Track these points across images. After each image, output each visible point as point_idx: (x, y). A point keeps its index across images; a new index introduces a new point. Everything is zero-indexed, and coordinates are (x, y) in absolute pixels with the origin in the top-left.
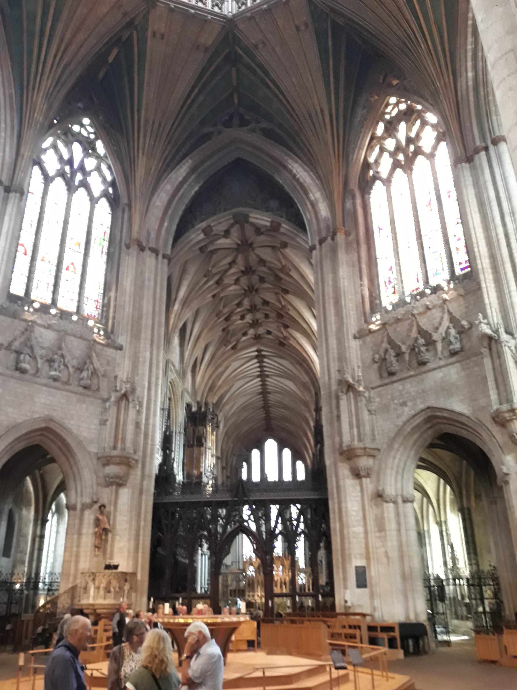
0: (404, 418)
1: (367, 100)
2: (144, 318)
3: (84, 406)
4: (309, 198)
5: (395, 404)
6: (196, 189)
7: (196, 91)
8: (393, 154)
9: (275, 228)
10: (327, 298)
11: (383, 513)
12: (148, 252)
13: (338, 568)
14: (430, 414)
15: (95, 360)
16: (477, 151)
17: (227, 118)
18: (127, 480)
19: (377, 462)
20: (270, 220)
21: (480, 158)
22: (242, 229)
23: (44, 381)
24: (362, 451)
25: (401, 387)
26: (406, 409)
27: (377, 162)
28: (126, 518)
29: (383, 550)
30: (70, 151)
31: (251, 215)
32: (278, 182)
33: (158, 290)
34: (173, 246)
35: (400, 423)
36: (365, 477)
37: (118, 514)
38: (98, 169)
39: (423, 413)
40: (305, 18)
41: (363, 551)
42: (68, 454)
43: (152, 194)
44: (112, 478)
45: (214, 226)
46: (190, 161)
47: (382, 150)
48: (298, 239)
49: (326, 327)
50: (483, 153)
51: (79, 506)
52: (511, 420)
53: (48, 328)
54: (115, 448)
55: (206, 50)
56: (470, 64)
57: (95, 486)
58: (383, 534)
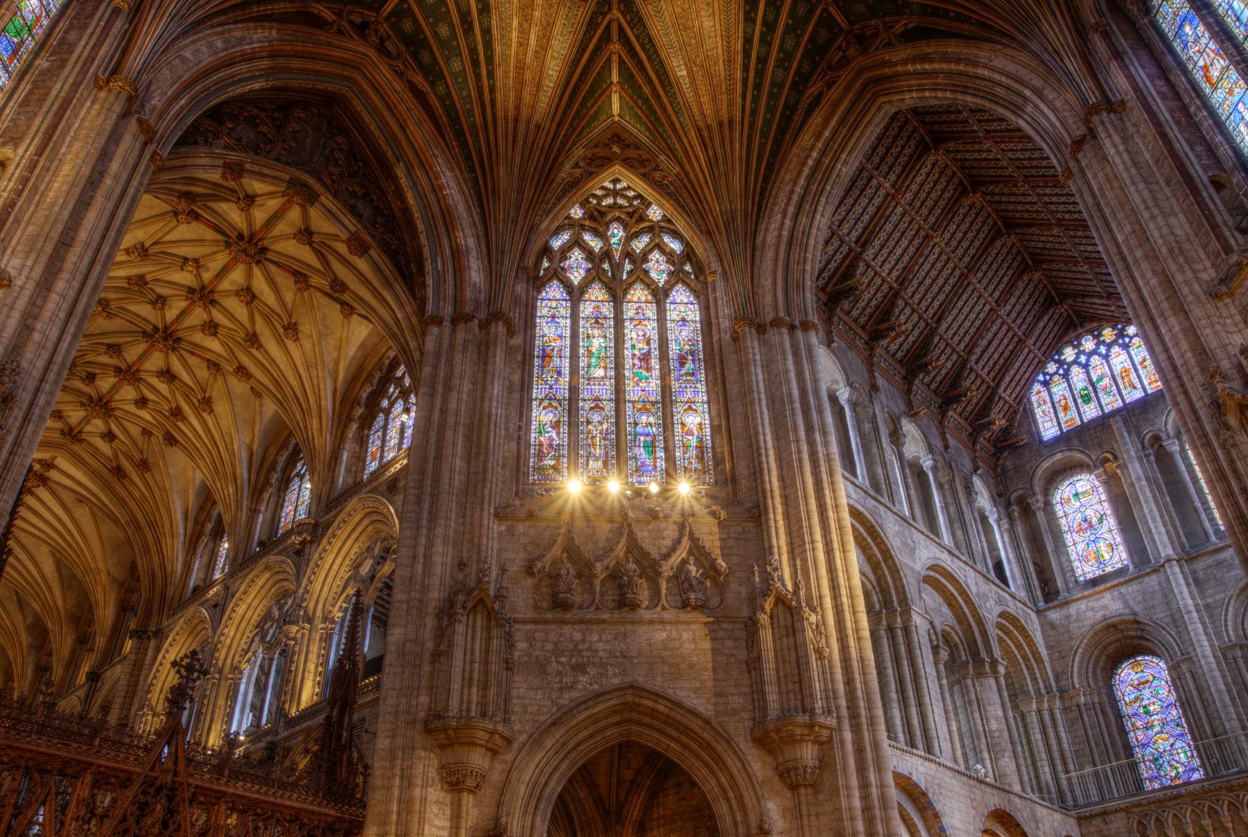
5: (558, 662)
6: (257, 86)
10: (451, 420)
14: (629, 698)
16: (777, 323)
17: (358, 20)
19: (498, 767)
21: (781, 334)
24: (486, 736)
26: (584, 679)
35: (565, 699)
36: (471, 791)
39: (617, 694)
46: (274, 32)
50: (785, 330)
52: (801, 741)
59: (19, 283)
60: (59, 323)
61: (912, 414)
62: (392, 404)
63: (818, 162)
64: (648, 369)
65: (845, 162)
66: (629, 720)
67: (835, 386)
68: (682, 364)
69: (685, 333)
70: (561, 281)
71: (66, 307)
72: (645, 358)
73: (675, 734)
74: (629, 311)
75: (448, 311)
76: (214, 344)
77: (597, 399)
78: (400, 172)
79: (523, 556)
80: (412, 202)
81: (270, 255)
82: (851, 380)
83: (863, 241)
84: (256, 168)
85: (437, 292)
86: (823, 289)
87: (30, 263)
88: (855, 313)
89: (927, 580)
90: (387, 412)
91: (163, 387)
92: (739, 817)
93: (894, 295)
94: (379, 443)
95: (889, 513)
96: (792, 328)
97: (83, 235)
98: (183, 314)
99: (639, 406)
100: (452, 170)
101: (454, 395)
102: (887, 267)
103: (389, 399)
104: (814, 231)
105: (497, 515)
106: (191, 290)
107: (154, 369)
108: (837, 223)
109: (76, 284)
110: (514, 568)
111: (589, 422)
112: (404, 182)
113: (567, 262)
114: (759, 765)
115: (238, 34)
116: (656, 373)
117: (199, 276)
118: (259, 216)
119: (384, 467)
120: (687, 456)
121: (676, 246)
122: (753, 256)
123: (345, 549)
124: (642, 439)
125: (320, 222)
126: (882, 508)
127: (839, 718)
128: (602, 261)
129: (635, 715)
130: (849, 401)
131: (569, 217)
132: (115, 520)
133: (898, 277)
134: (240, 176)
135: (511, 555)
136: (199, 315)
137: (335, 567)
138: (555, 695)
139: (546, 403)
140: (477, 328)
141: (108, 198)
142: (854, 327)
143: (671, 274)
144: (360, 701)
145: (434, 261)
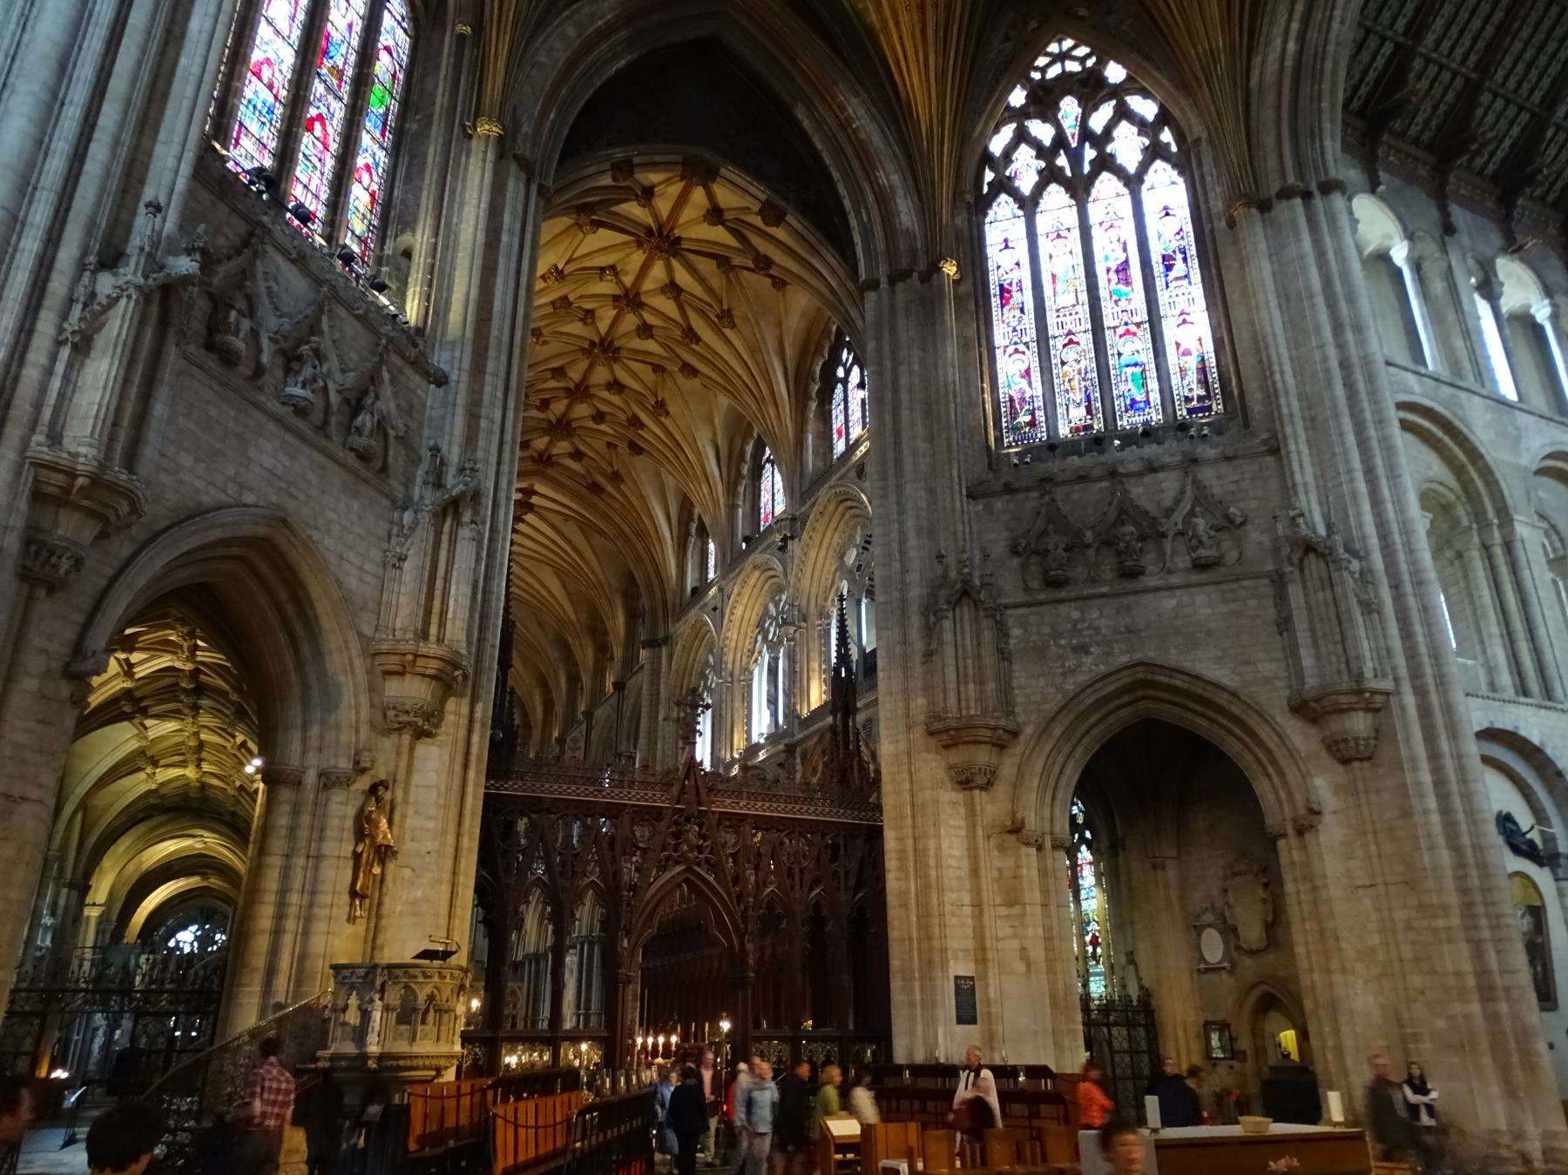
0: (1082, 678)
3: (356, 506)
5: (1058, 646)
6: (622, 63)
10: (905, 397)
11: (1018, 867)
13: (908, 979)
14: (1141, 676)
15: (387, 390)
16: (1286, 194)
18: (437, 726)
20: (763, 197)
21: (1292, 209)
23: (275, 406)
25: (1076, 615)
26: (1087, 661)
28: (431, 825)
29: (1015, 944)
31: (723, 171)
35: (1070, 686)
36: (983, 788)
37: (410, 811)
39: (1128, 672)
41: (970, 944)
42: (299, 629)
44: (407, 712)
50: (1298, 202)
51: (311, 778)
53: (293, 262)
54: (424, 634)
57: (364, 729)
58: (1016, 910)
59: (453, 377)
60: (499, 403)
61: (1512, 247)
62: (848, 372)
66: (1143, 698)
67: (1387, 243)
68: (1169, 268)
69: (1171, 225)
70: (1010, 194)
71: (501, 385)
72: (1123, 269)
73: (1199, 708)
74: (1095, 212)
75: (882, 271)
76: (651, 346)
77: (1070, 333)
78: (800, 113)
79: (1005, 534)
80: (819, 146)
81: (685, 245)
82: (1411, 228)
83: (1416, 29)
84: (645, 159)
85: (867, 252)
86: (1360, 114)
87: (457, 354)
88: (1413, 130)
89: (1541, 472)
90: (845, 382)
91: (615, 399)
92: (1283, 795)
93: (1473, 90)
94: (841, 417)
95: (1476, 399)
96: (1307, 196)
97: (497, 305)
98: (615, 321)
99: (1121, 330)
100: (857, 95)
101: (904, 368)
102: (1459, 51)
103: (844, 366)
104: (1331, 48)
105: (968, 496)
106: (616, 298)
107: (602, 382)
108: (1372, 15)
109: (504, 358)
110: (999, 549)
111: (1063, 363)
112: (807, 124)
113: (1013, 167)
114: (1300, 736)
115: (587, 10)
117: (620, 282)
118: (664, 206)
119: (851, 448)
121: (1146, 108)
122: (1247, 105)
123: (826, 541)
124: (1130, 370)
125: (726, 197)
126: (1463, 395)
127: (1396, 680)
128: (1056, 154)
129: (1151, 692)
130: (1409, 259)
131: (1008, 108)
132: (601, 532)
133: (1478, 63)
134: (631, 173)
135: (993, 536)
136: (630, 321)
137: (820, 560)
138: (1058, 680)
139: (1011, 349)
140: (918, 283)
141: (509, 257)
142: (1413, 150)
143: (1145, 150)
144: (859, 705)
145: (858, 215)
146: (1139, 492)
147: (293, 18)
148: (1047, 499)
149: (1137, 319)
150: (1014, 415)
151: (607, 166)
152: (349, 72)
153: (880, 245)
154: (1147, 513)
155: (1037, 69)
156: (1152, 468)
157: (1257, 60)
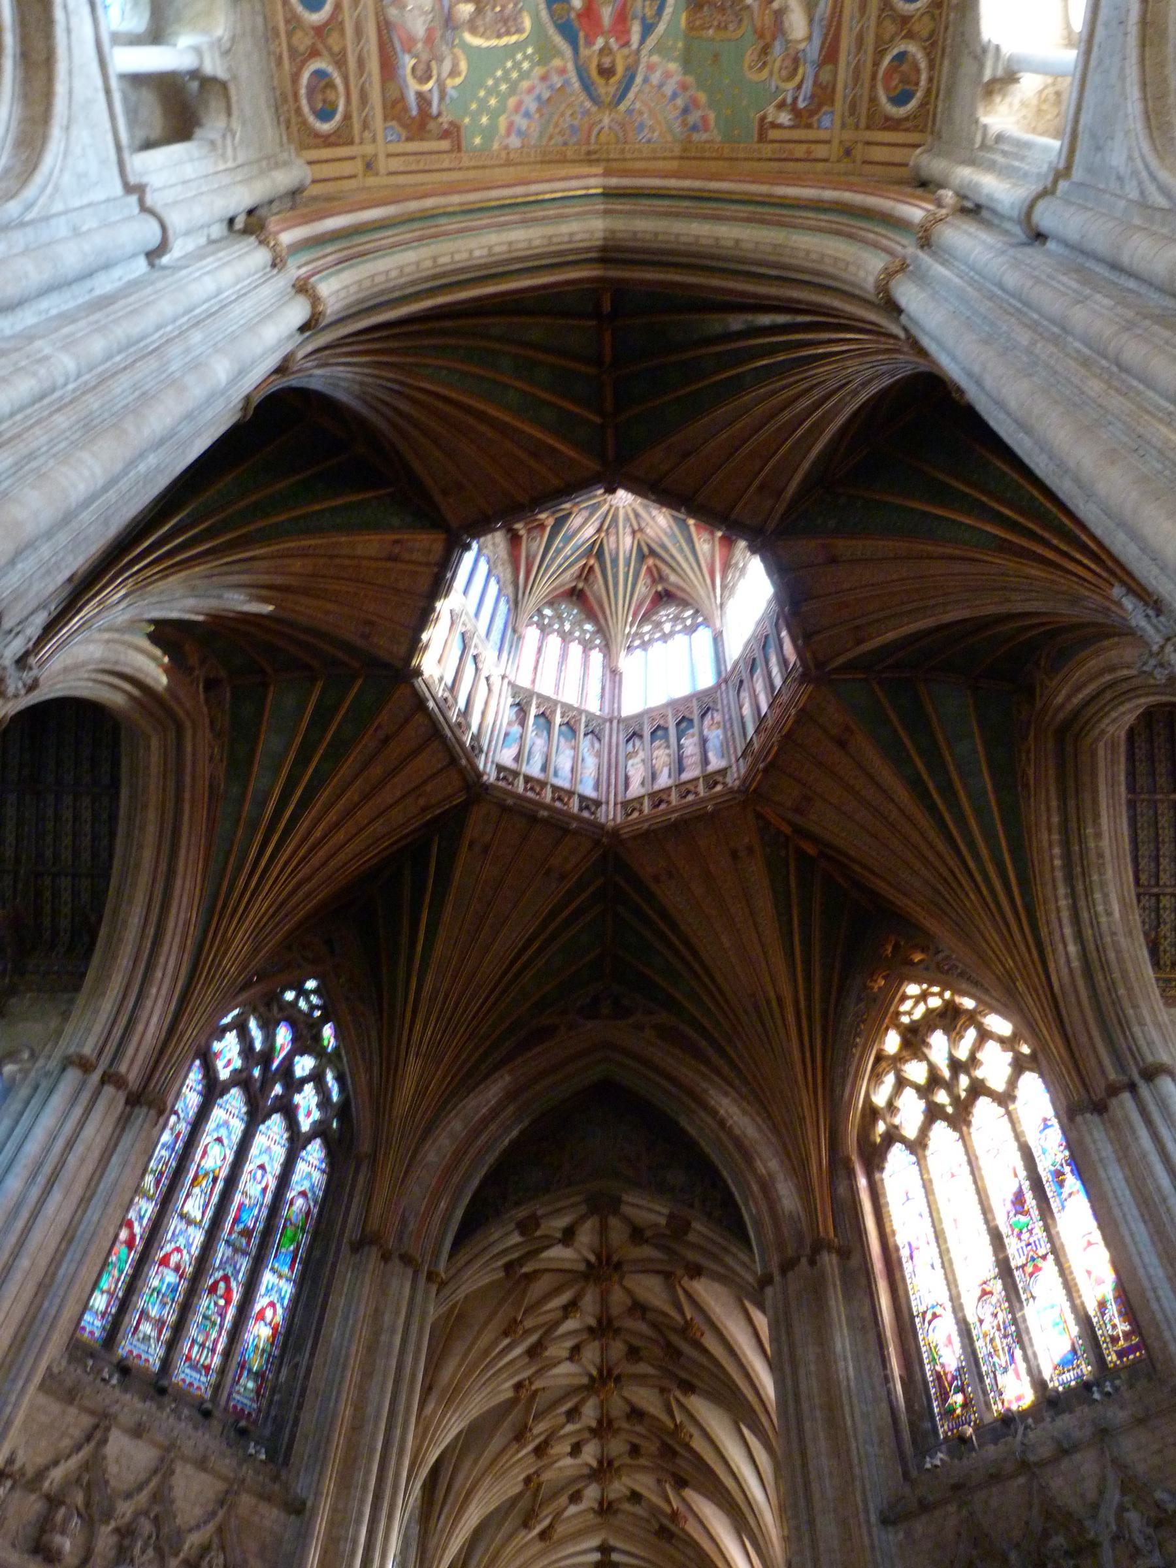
1: (865, 987)
2: (369, 1428)
4: (754, 1170)
6: (515, 1133)
7: (536, 944)
8: (925, 1092)
9: (679, 1227)
12: (396, 1265)
16: (1113, 1090)
20: (666, 1211)
21: (1122, 1106)
22: (603, 1229)
27: (891, 1107)
30: (270, 1038)
31: (625, 1197)
32: (684, 1132)
33: (409, 1360)
34: (451, 1255)
38: (316, 1077)
40: (747, 840)
43: (423, 1139)
45: (545, 1216)
46: (508, 1078)
47: (901, 1083)
48: (729, 1260)
49: (807, 1485)
50: (1126, 1096)
55: (563, 877)
56: (1068, 931)
63: (1067, 856)
64: (1027, 1213)
65: (1098, 835)
68: (1061, 1184)
78: (684, 1122)
84: (549, 1208)
96: (1132, 1087)
100: (726, 1094)
115: (473, 1103)
116: (1035, 1213)
120: (1107, 1318)
146: (1057, 1484)
147: (206, 1206)
148: (964, 1512)
149: (1041, 1252)
150: (944, 1396)
151: (512, 1226)
152: (260, 1226)
153: (770, 1235)
154: (1069, 1514)
155: (905, 1013)
156: (1065, 1450)
157: (1052, 966)
